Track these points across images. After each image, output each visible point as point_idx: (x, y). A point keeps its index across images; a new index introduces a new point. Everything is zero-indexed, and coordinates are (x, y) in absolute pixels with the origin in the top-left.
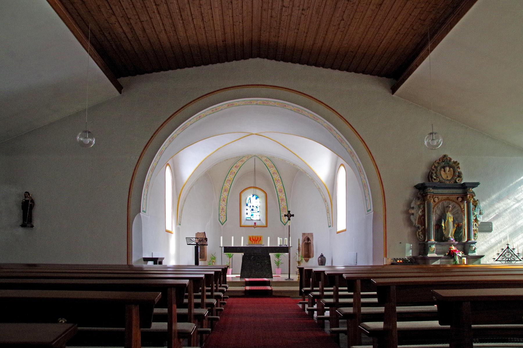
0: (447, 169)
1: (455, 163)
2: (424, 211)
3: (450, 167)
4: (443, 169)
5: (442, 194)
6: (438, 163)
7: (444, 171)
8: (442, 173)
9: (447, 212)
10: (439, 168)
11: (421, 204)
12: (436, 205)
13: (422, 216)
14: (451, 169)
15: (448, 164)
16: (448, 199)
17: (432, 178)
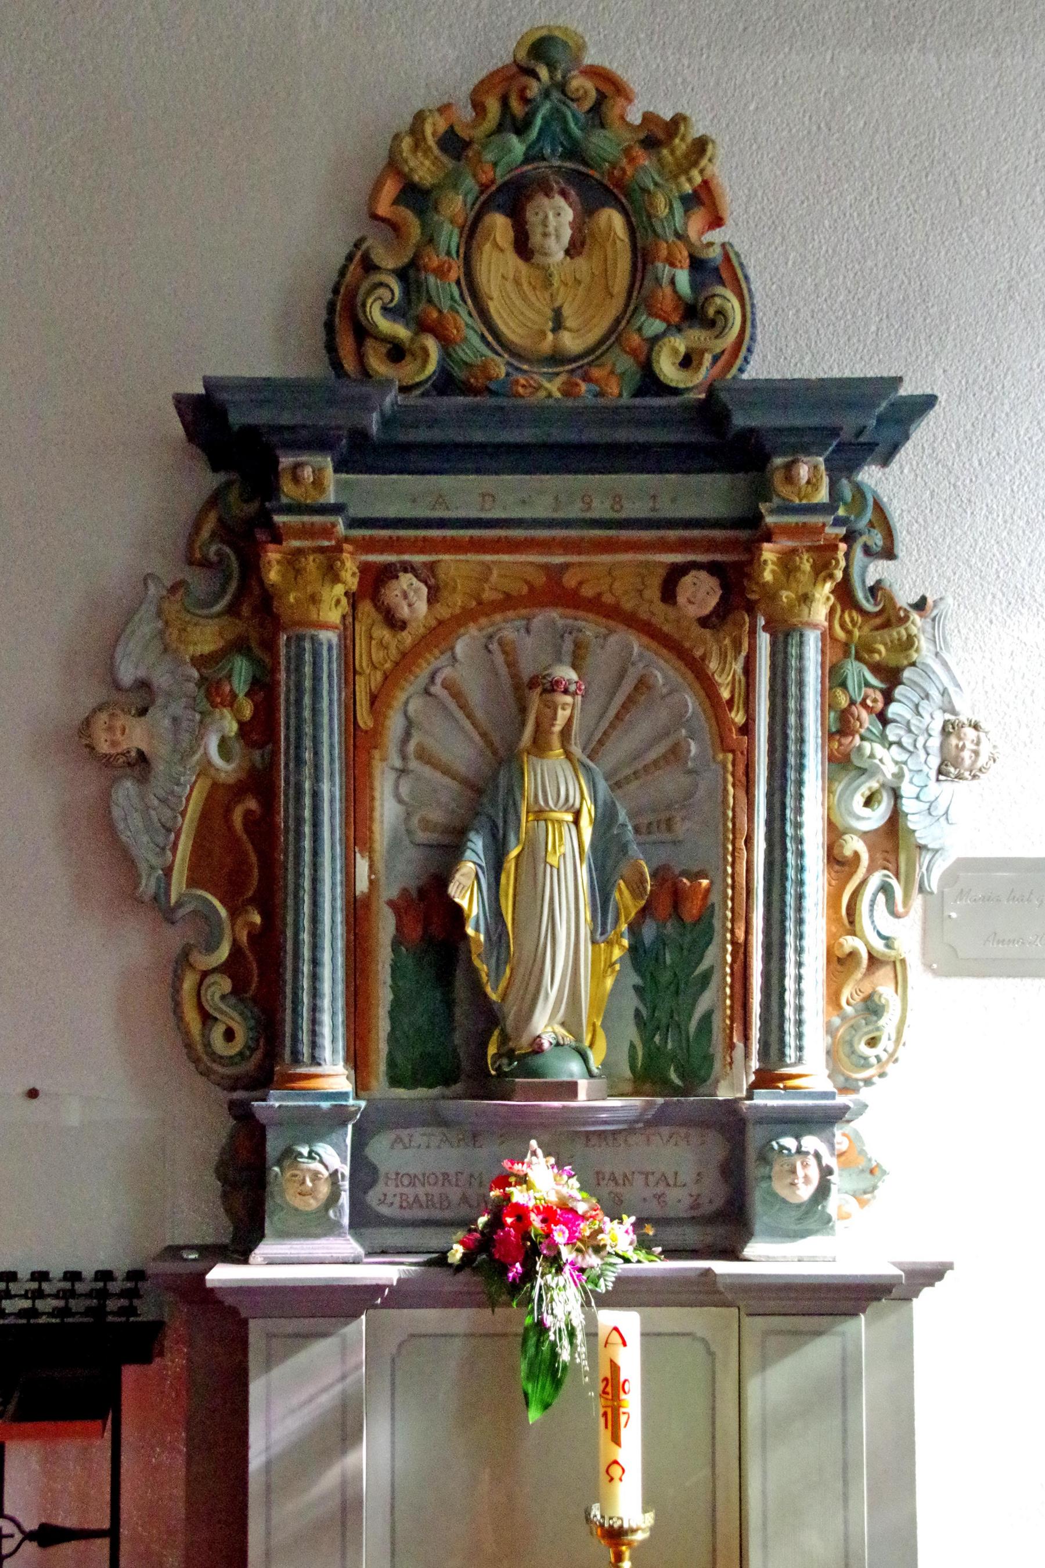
0: (557, 217)
1: (658, 134)
2: (260, 731)
3: (595, 190)
4: (500, 224)
5: (484, 533)
6: (453, 144)
7: (523, 247)
8: (497, 265)
9: (540, 746)
10: (456, 205)
11: (239, 646)
12: (406, 661)
13: (238, 790)
14: (613, 220)
15: (574, 151)
16: (554, 592)
17: (362, 332)
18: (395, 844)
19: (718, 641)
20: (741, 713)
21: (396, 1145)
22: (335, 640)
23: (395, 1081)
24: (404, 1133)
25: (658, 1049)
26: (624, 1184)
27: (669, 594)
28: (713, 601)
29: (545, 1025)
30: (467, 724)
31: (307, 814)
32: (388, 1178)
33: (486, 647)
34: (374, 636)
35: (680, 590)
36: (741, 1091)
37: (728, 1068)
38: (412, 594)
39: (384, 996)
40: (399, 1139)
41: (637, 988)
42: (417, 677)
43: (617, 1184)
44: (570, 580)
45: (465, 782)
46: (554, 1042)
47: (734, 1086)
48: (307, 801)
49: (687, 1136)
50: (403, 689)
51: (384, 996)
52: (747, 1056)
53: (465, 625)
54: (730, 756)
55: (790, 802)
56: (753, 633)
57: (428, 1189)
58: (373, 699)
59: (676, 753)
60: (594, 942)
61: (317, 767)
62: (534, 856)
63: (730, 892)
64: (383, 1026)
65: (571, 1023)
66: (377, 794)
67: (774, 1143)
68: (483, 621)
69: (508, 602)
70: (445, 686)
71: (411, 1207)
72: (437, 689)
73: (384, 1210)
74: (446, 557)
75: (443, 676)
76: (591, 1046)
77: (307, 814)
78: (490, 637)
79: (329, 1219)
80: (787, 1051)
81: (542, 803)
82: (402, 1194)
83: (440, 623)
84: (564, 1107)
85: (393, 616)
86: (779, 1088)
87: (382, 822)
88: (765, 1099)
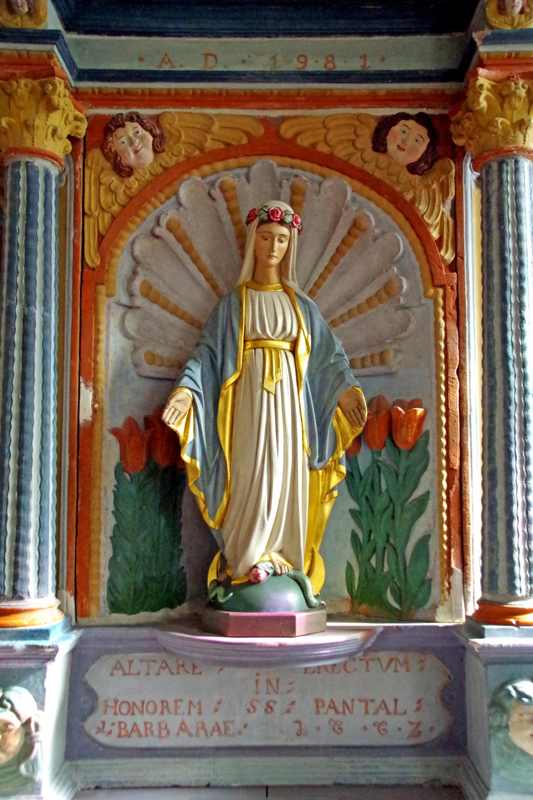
5: (207, 87)
9: (258, 281)
12: (133, 205)
16: (272, 143)
18: (120, 375)
19: (428, 187)
20: (450, 251)
21: (115, 672)
22: (54, 172)
23: (115, 607)
24: (124, 659)
25: (374, 571)
26: (344, 713)
27: (379, 144)
28: (422, 148)
29: (261, 553)
30: (193, 268)
31: (17, 338)
32: (107, 706)
33: (209, 194)
34: (102, 181)
35: (389, 138)
36: (459, 616)
37: (446, 593)
38: (138, 141)
39: (106, 522)
40: (118, 666)
41: (352, 512)
42: (143, 220)
43: (337, 712)
44: (287, 131)
45: (192, 322)
46: (271, 572)
47: (454, 612)
48: (18, 324)
49: (406, 662)
50: (128, 230)
51: (106, 522)
52: (465, 580)
53: (188, 171)
54: (441, 291)
55: (511, 325)
56: (459, 178)
57: (147, 717)
58: (101, 238)
59: (388, 290)
60: (312, 468)
61: (29, 291)
62: (251, 385)
63: (444, 419)
64: (104, 552)
65: (288, 551)
66: (102, 327)
67: (510, 688)
68: (206, 168)
69: (228, 151)
70: (169, 228)
71: (129, 736)
72: (161, 231)
73: (102, 738)
74: (171, 110)
75: (168, 217)
76: (309, 574)
77: (17, 338)
78: (212, 184)
79: (20, 775)
80: (517, 583)
81: (260, 332)
82: (120, 723)
83: (165, 169)
84: (281, 646)
85: (120, 161)
86: (511, 624)
87: (107, 354)
88: (496, 637)
